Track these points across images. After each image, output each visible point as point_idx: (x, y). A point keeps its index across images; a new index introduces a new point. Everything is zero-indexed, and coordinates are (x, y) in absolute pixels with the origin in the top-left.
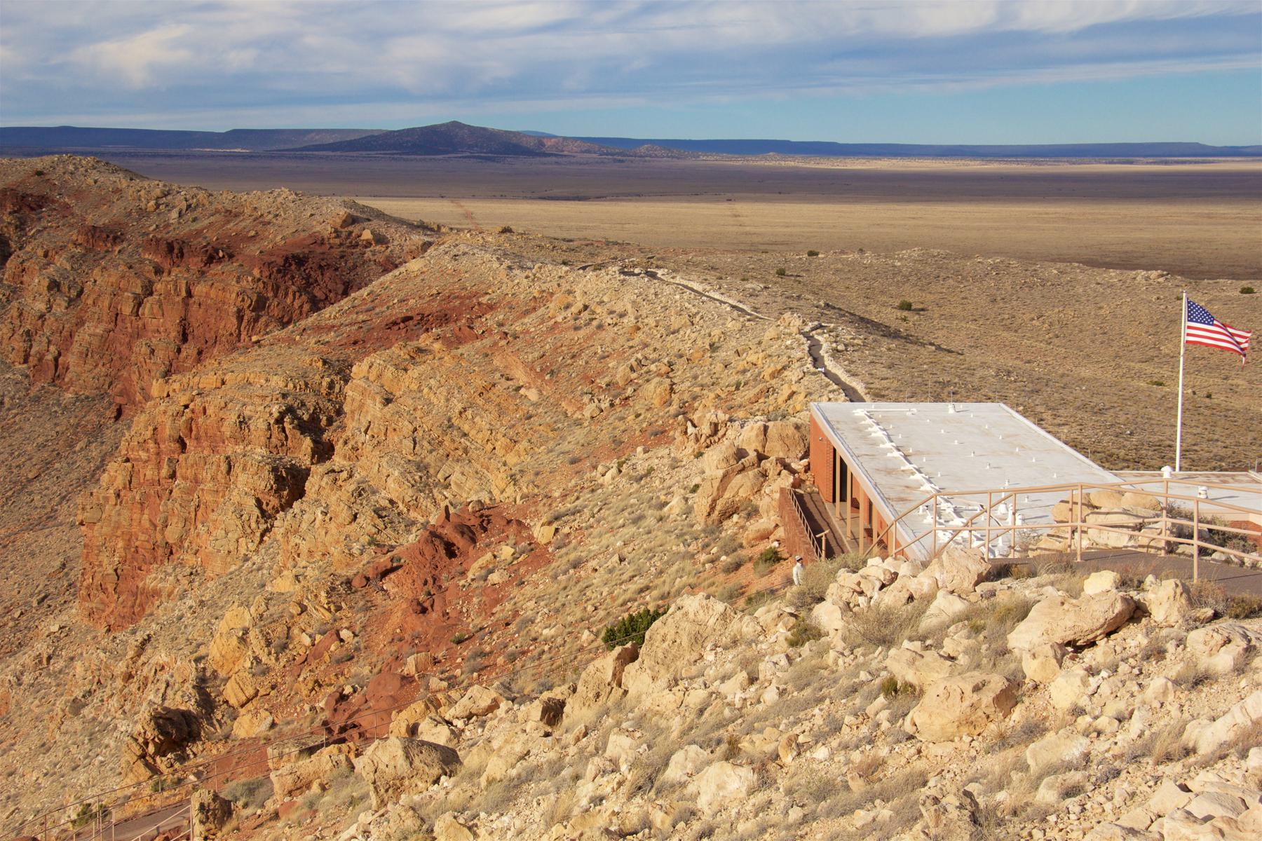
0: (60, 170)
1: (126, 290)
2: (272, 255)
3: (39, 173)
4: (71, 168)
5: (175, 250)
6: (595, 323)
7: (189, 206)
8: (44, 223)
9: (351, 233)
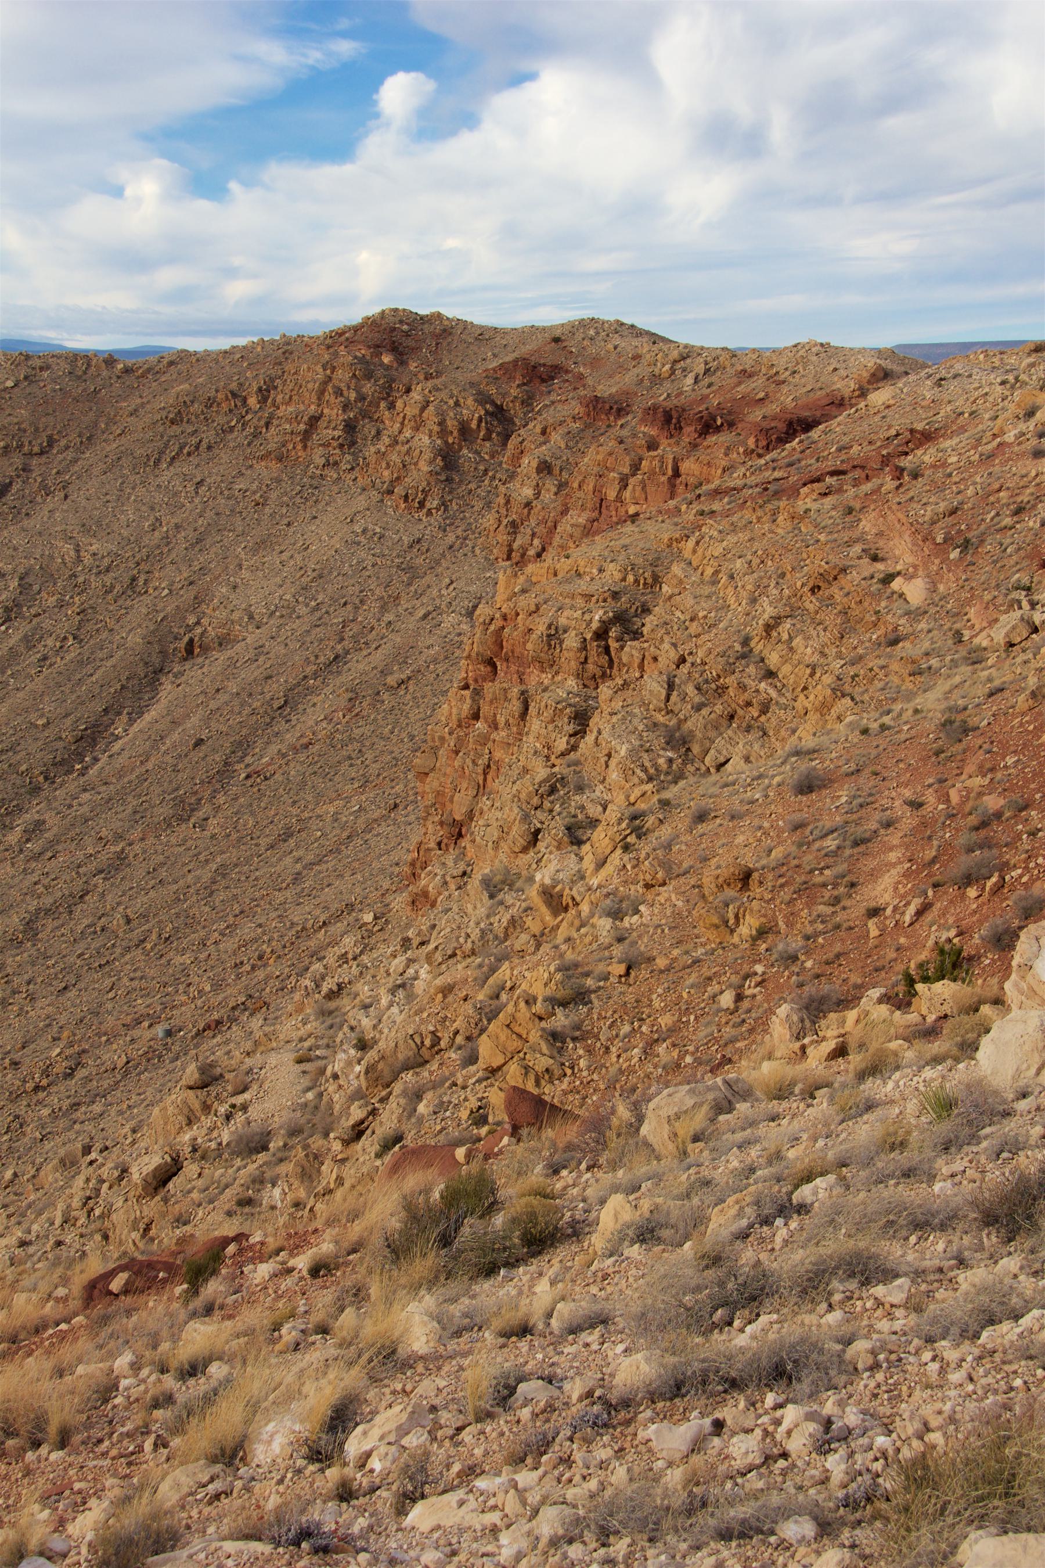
0: (579, 336)
1: (613, 470)
3: (557, 340)
4: (592, 332)
5: (670, 420)
7: (707, 371)
8: (553, 397)
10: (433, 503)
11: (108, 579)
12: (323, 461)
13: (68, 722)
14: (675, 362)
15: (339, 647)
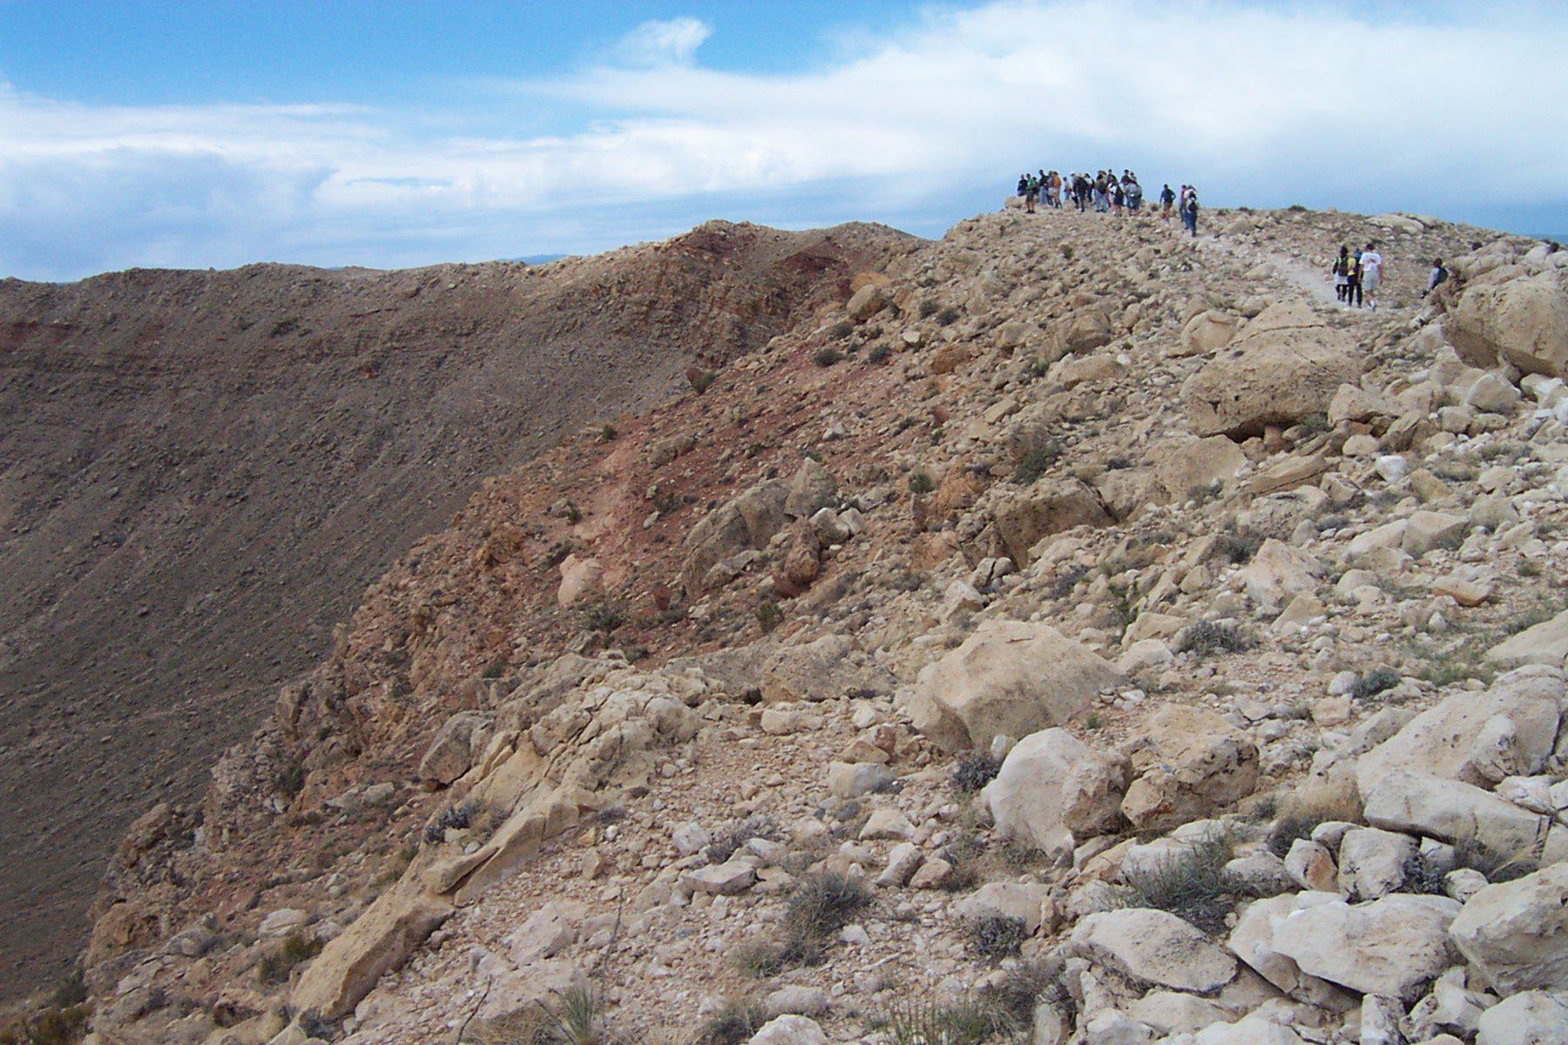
3: (828, 239)
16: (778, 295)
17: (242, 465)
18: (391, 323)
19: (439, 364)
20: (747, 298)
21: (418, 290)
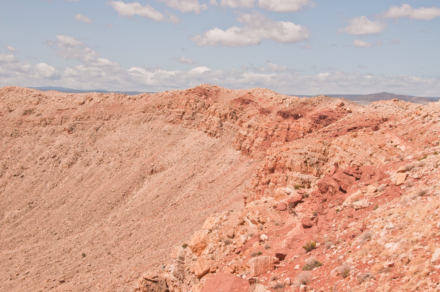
0: (255, 92)
2: (316, 115)
3: (250, 93)
6: (432, 121)
8: (249, 108)
9: (342, 109)
10: (218, 134)
11: (128, 153)
12: (187, 123)
13: (120, 190)
14: (283, 100)
15: (194, 172)
16: (234, 112)
17: (18, 164)
18: (75, 114)
19: (97, 130)
20: (223, 112)
21: (84, 102)
